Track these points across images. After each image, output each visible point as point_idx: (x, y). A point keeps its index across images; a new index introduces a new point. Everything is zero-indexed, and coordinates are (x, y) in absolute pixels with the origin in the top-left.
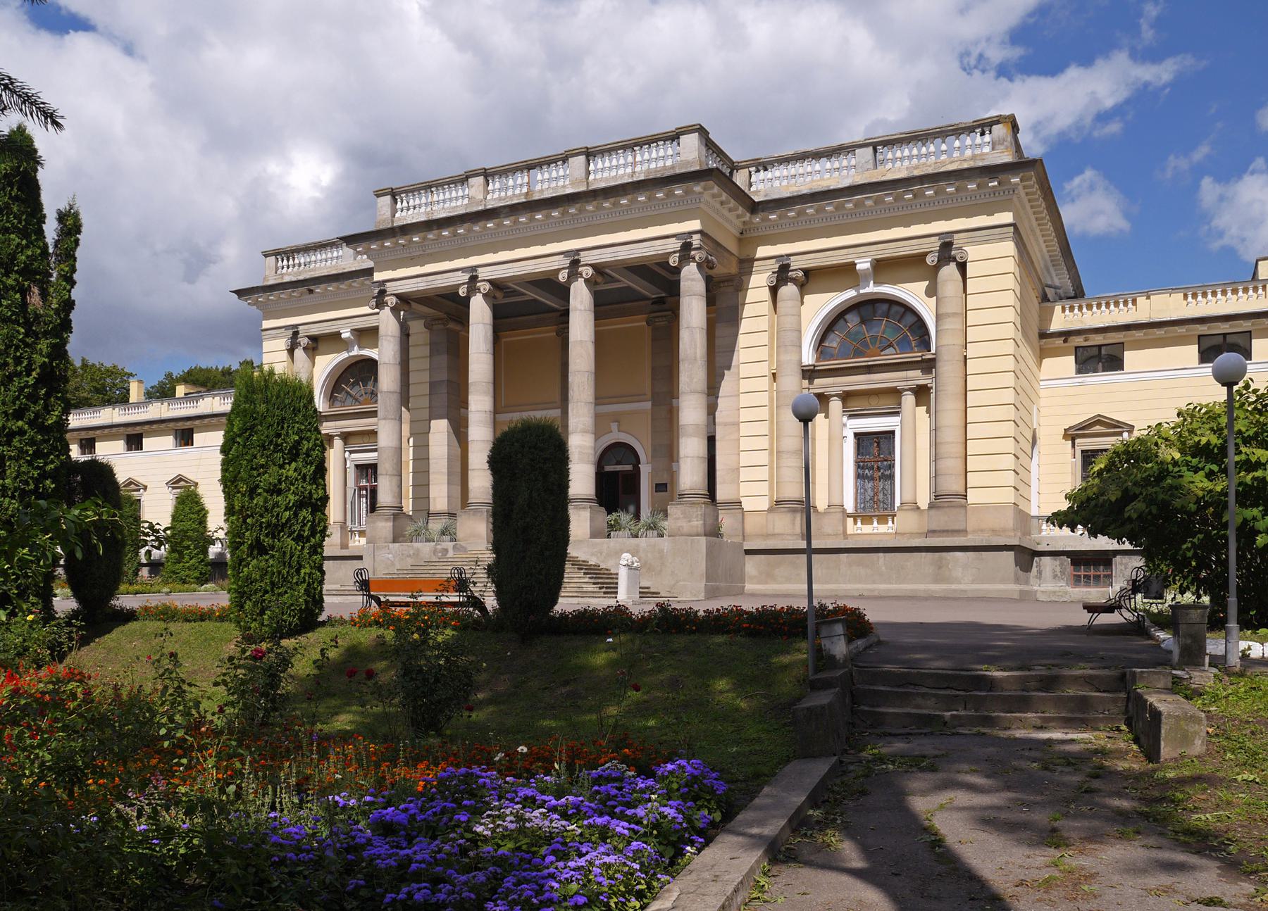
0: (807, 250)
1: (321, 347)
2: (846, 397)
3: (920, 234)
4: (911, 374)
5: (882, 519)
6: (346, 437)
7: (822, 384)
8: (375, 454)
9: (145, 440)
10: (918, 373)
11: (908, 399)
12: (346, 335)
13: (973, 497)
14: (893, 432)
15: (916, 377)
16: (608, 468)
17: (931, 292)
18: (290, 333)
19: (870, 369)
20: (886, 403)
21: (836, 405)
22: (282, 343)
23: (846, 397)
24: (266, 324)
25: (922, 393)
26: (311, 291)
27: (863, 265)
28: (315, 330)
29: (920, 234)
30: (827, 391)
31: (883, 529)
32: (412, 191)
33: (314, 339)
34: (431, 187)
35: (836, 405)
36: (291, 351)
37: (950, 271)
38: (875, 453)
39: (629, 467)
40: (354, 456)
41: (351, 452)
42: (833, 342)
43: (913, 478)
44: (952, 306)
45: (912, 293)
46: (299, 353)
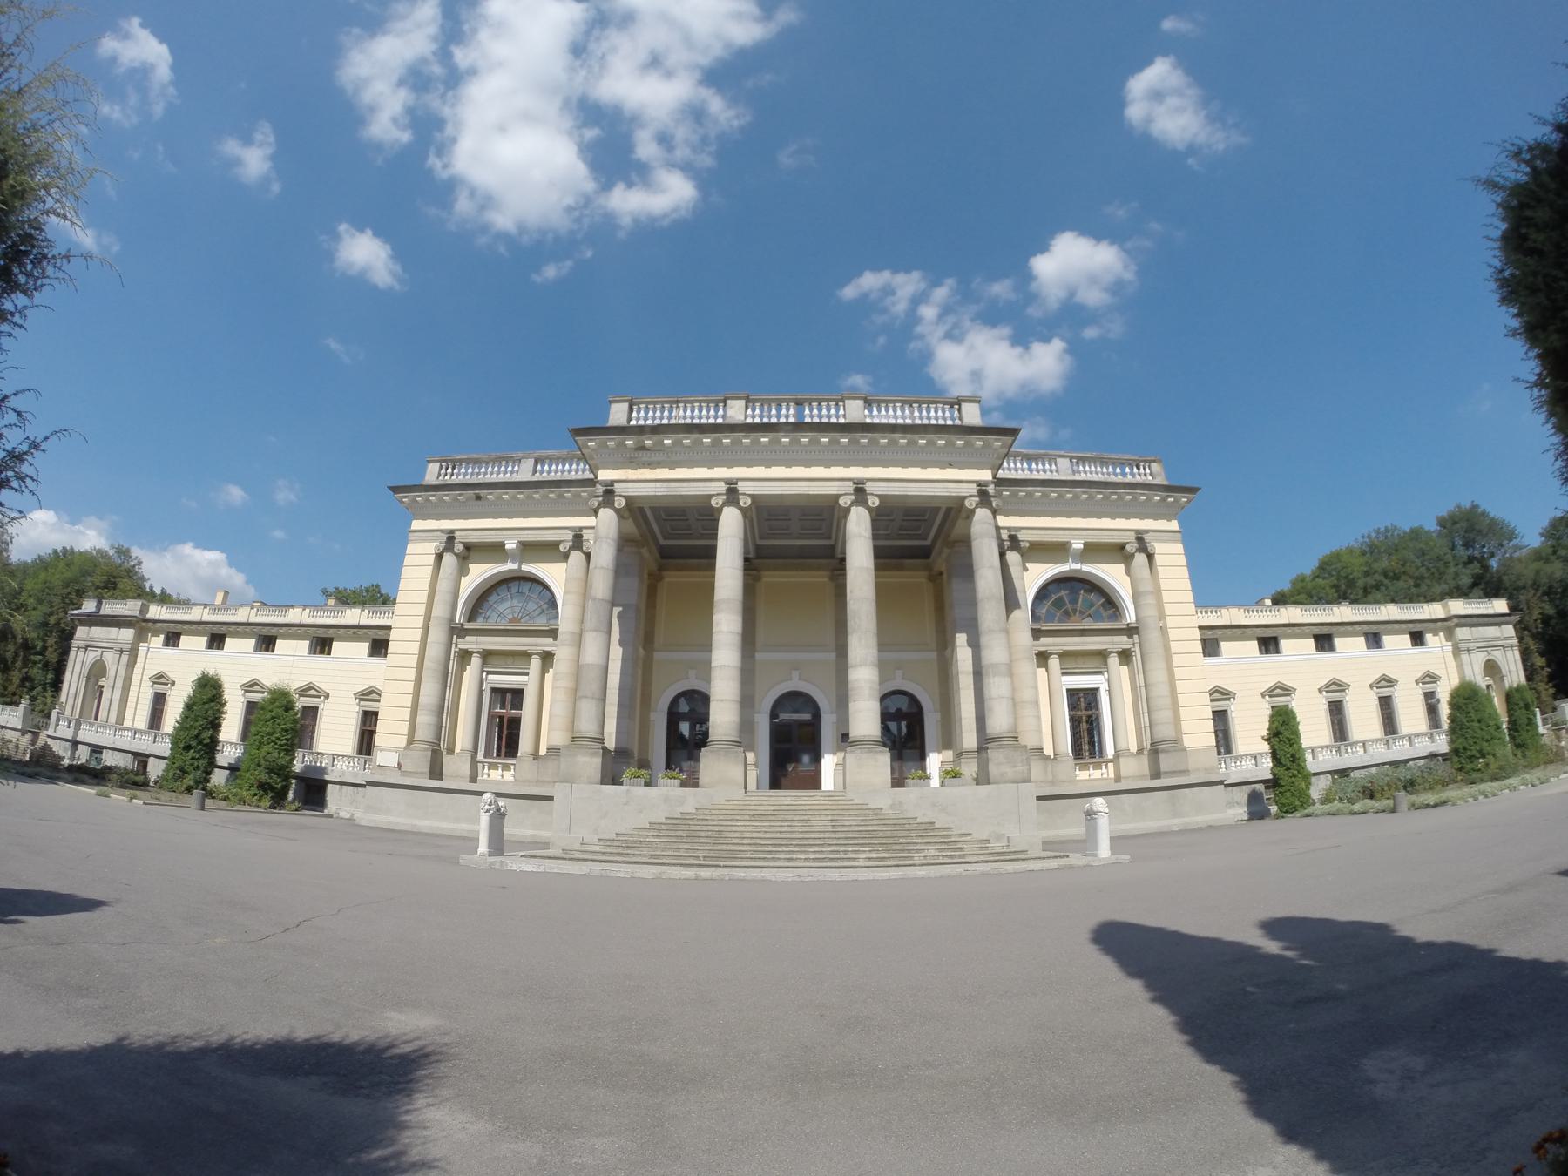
0: (1031, 525)
1: (473, 555)
2: (1063, 656)
3: (1120, 527)
4: (1116, 639)
5: (1098, 766)
6: (487, 656)
7: (1046, 643)
8: (524, 678)
9: (228, 640)
11: (1113, 660)
12: (511, 545)
13: (1188, 742)
14: (1097, 690)
15: (1122, 642)
16: (783, 716)
17: (1128, 572)
18: (444, 537)
19: (1083, 633)
20: (1092, 664)
21: (1054, 662)
22: (431, 548)
23: (1063, 656)
24: (417, 524)
25: (1125, 656)
27: (1078, 545)
28: (473, 538)
29: (1120, 527)
30: (1050, 649)
31: (1096, 774)
33: (468, 547)
35: (1054, 662)
36: (439, 557)
37: (1140, 559)
38: (1084, 707)
39: (807, 717)
40: (491, 677)
41: (489, 673)
42: (1043, 611)
43: (1120, 727)
44: (1146, 586)
45: (1111, 574)
46: (449, 559)
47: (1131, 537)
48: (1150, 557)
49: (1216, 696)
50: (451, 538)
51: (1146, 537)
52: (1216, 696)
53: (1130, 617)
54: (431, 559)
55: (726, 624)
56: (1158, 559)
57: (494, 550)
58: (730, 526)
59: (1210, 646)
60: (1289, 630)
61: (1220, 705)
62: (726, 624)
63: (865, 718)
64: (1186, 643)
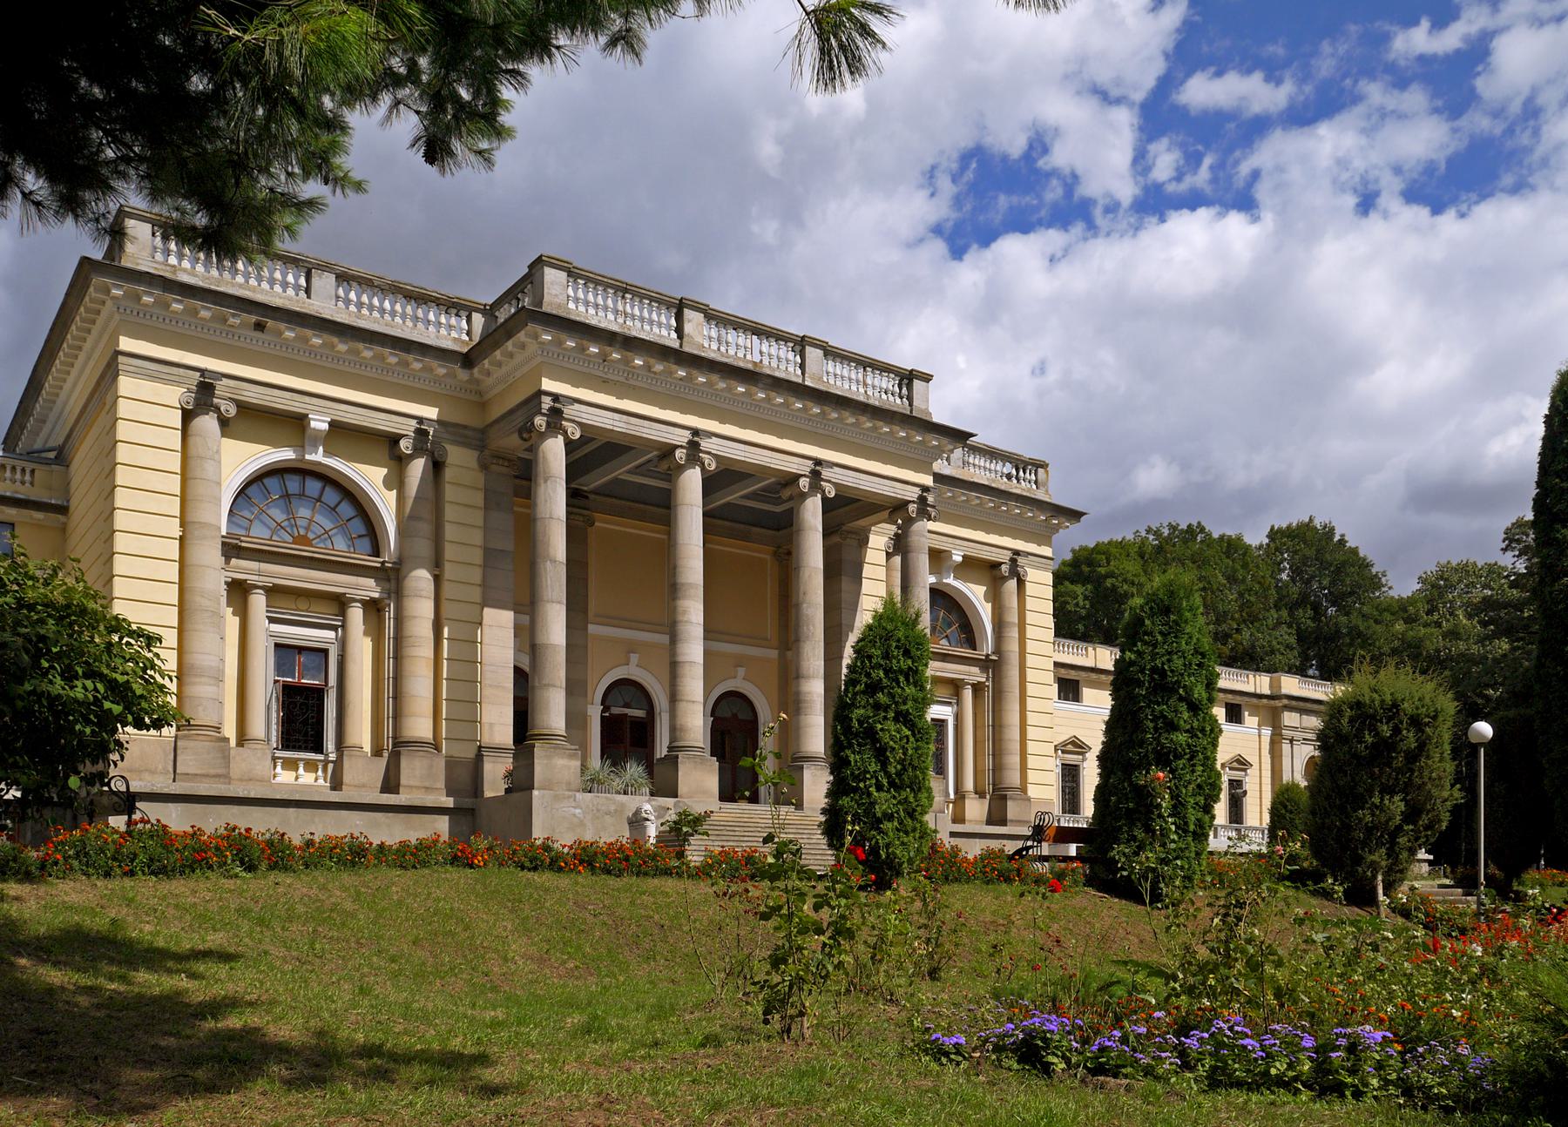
10: (976, 670)
12: (319, 424)
22: (175, 395)
26: (259, 327)
28: (253, 395)
32: (597, 283)
33: (244, 408)
34: (626, 291)
36: (188, 416)
47: (1005, 557)
48: (1021, 583)
49: (1070, 747)
50: (205, 389)
51: (1021, 560)
52: (1070, 747)
53: (987, 647)
54: (176, 419)
55: (693, 612)
56: (1030, 589)
57: (292, 425)
58: (691, 484)
59: (1069, 689)
60: (1094, 676)
61: (1072, 759)
62: (693, 612)
63: (696, 722)
64: (1042, 686)
